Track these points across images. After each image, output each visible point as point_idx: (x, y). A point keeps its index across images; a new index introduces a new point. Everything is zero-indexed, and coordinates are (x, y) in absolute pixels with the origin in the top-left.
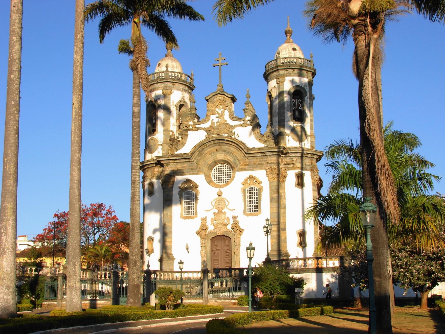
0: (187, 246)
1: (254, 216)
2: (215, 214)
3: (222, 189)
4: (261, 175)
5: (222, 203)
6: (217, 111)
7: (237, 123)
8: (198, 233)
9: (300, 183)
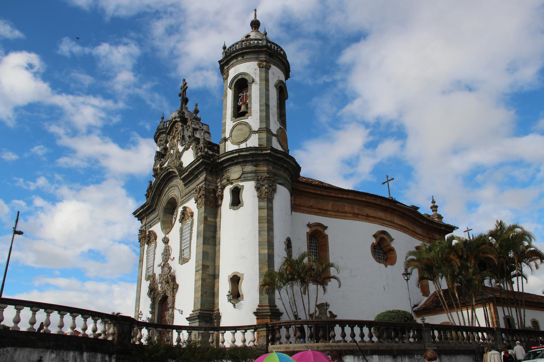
9: (236, 202)
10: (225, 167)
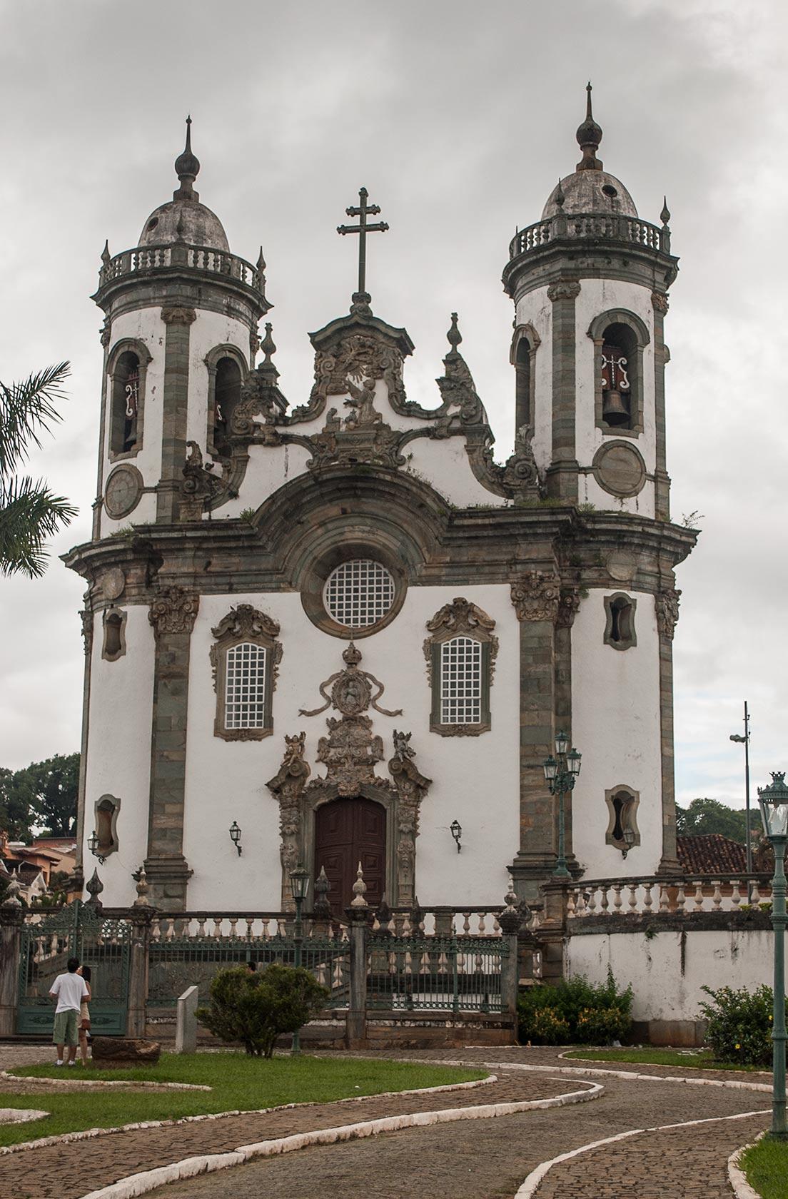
0: (235, 831)
1: (465, 738)
2: (332, 724)
3: (359, 644)
4: (493, 599)
5: (361, 690)
6: (349, 384)
7: (417, 424)
8: (275, 788)
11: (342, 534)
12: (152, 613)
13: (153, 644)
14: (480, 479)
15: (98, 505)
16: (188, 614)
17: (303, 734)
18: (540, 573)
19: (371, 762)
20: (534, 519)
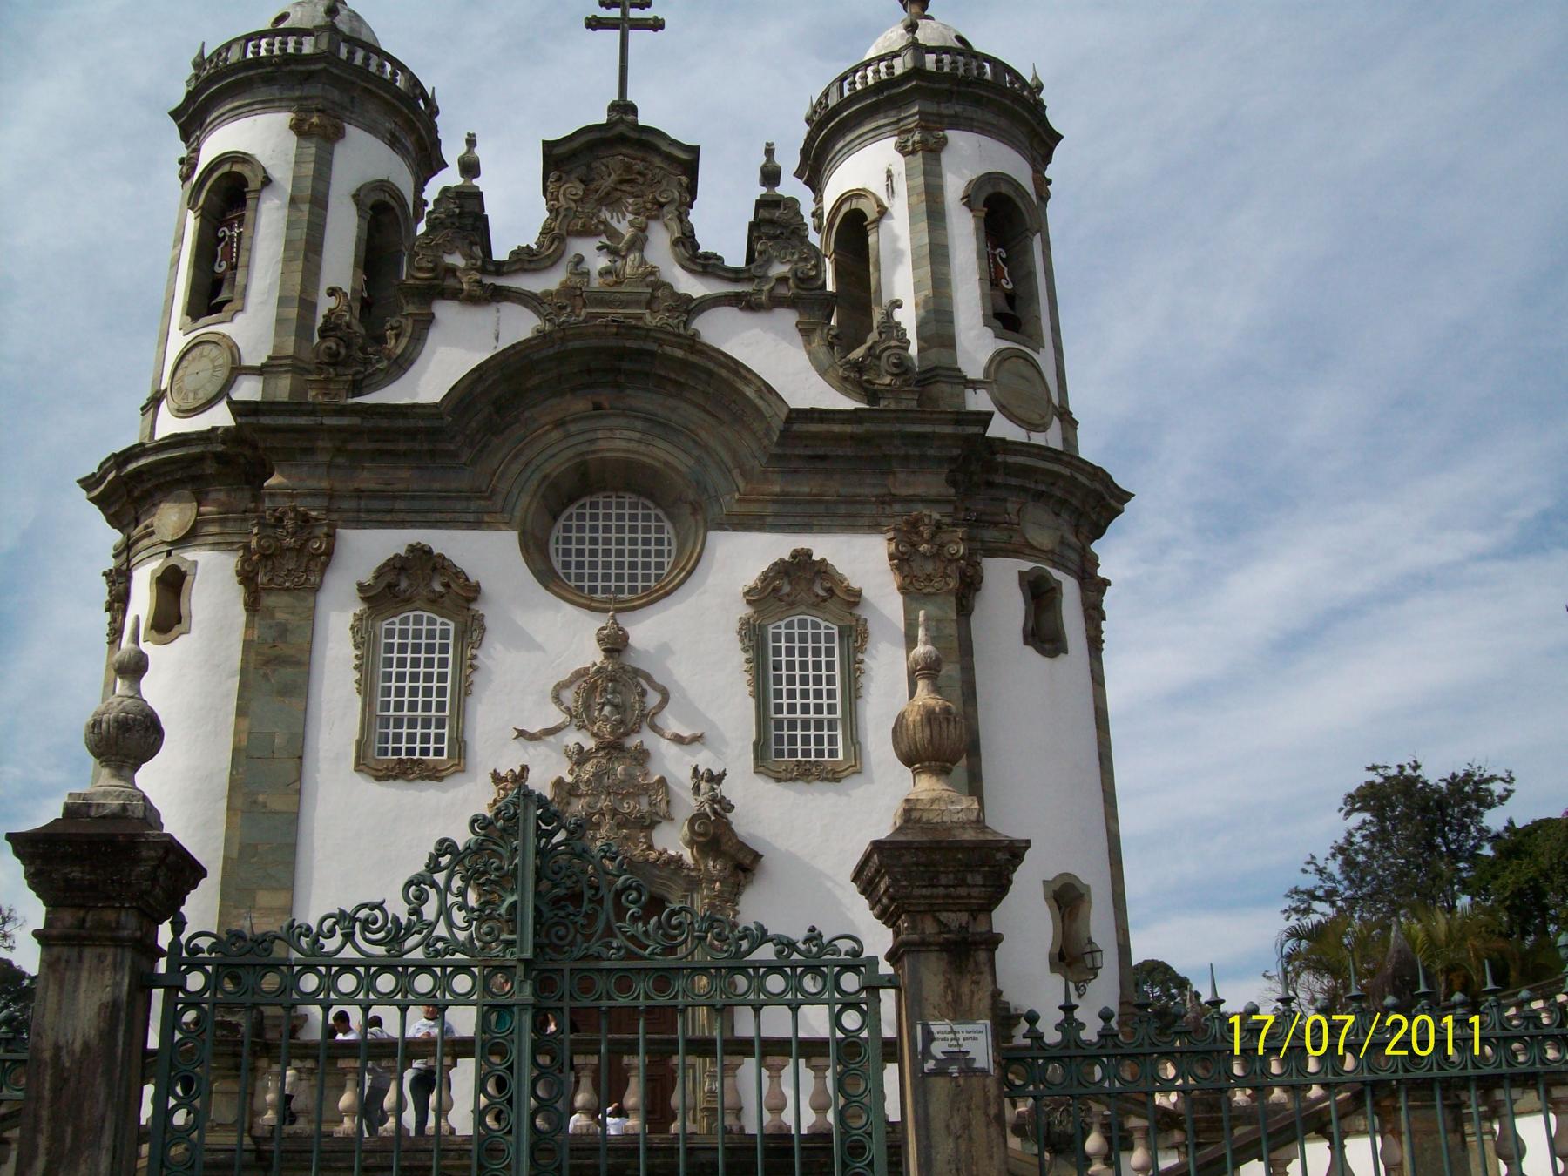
3: (622, 619)
6: (606, 224)
10: (990, 484)
11: (592, 441)
12: (245, 560)
13: (240, 615)
14: (823, 373)
15: (155, 401)
16: (315, 555)
17: (525, 769)
18: (936, 516)
19: (647, 824)
20: (927, 429)
